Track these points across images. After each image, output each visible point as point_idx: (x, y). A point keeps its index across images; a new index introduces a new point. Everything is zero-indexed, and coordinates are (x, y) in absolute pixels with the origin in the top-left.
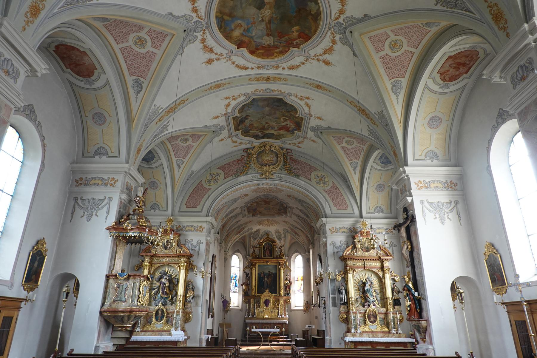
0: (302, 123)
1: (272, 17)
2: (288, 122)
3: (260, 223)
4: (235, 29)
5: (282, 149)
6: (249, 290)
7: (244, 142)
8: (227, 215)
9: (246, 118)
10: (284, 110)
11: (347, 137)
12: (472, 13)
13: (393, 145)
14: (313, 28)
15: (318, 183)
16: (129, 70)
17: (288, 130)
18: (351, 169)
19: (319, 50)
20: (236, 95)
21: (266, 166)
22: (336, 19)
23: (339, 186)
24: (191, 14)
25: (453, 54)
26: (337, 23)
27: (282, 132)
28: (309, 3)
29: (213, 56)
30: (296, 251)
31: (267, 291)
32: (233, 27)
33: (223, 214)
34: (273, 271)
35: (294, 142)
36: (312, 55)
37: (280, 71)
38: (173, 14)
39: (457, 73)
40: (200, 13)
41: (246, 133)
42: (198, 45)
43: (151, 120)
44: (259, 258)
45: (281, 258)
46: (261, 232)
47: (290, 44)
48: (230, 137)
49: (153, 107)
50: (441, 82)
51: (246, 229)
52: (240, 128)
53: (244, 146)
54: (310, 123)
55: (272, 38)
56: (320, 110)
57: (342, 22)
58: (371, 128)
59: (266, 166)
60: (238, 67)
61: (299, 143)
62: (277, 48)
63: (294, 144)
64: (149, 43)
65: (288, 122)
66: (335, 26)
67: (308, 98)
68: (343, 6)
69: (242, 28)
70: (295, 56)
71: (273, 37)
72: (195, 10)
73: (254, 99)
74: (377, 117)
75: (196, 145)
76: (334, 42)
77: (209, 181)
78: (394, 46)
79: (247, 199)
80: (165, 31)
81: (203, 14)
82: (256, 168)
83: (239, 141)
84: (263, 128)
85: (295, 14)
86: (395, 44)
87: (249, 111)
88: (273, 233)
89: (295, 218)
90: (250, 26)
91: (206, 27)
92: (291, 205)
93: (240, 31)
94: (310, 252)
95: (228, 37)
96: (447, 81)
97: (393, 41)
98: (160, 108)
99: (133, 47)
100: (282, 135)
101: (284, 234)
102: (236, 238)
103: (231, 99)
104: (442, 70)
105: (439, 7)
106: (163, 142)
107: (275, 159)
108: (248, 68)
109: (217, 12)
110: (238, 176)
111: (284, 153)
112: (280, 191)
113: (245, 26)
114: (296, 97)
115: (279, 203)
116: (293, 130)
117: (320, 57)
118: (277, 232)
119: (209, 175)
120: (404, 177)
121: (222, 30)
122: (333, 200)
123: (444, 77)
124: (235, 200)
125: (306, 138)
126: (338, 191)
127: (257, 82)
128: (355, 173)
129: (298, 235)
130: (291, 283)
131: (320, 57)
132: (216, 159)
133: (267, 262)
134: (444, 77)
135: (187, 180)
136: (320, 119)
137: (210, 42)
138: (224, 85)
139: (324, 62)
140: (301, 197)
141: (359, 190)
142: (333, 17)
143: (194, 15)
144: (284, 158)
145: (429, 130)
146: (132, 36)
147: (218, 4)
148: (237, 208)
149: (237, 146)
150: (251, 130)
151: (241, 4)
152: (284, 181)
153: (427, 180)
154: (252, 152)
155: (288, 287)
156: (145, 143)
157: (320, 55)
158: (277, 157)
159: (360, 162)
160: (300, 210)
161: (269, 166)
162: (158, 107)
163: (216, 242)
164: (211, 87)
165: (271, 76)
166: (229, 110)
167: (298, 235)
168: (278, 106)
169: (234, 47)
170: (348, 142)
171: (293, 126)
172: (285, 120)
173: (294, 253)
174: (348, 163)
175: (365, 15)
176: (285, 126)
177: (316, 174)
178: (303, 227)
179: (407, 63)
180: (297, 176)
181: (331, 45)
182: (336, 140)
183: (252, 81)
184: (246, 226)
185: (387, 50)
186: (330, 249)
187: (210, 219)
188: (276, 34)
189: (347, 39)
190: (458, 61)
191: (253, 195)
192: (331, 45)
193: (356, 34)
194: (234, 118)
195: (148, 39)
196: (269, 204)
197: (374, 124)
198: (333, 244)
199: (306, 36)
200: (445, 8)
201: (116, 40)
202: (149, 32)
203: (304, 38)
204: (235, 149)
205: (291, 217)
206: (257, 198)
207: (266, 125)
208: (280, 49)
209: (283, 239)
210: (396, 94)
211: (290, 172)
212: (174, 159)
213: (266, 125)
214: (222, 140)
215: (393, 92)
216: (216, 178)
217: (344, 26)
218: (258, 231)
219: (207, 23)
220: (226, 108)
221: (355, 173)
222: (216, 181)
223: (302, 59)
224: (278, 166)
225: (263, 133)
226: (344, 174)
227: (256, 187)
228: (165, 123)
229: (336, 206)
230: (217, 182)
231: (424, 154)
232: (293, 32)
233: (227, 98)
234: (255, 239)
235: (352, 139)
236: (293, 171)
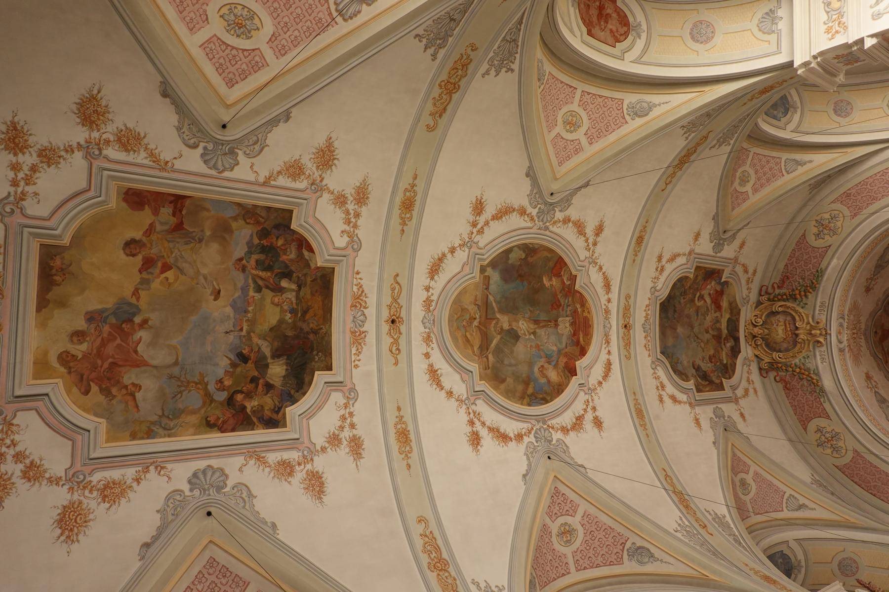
0: (705, 268)
1: (529, 318)
2: (705, 292)
4: (546, 377)
5: (759, 303)
7: (745, 375)
9: (698, 369)
10: (682, 301)
11: (732, 183)
12: (524, 13)
13: (749, 96)
14: (546, 254)
16: (611, 564)
17: (720, 293)
18: (801, 170)
19: (579, 243)
20: (655, 383)
21: (797, 335)
22: (532, 219)
23: (842, 190)
24: (525, 444)
25: (585, 30)
26: (538, 218)
27: (725, 304)
28: (510, 262)
29: (589, 416)
32: (543, 381)
35: (743, 282)
36: (587, 254)
37: (613, 307)
38: (525, 472)
39: (614, 15)
40: (524, 431)
41: (728, 370)
42: (571, 439)
43: (704, 543)
47: (570, 291)
48: (736, 401)
49: (679, 535)
50: (630, 38)
52: (717, 381)
53: (755, 376)
54: (707, 253)
55: (560, 319)
56: (682, 236)
57: (537, 210)
58: (715, 142)
59: (797, 335)
60: (606, 376)
61: (746, 271)
62: (575, 311)
63: (748, 282)
64: (568, 519)
65: (705, 292)
66: (542, 221)
67: (660, 258)
68: (514, 210)
69: (546, 365)
70: (589, 281)
71: (558, 317)
72: (519, 437)
73: (662, 353)
74: (693, 135)
75: (753, 468)
76: (566, 221)
77: (835, 449)
78: (572, 124)
79: (878, 376)
80: (550, 489)
81: (525, 425)
82: (804, 354)
83: (744, 384)
84: (718, 338)
85: (525, 283)
86: (569, 123)
87: (685, 363)
90: (542, 353)
91: (544, 424)
93: (550, 370)
95: (559, 389)
96: (629, 29)
97: (565, 127)
98: (680, 522)
99: (574, 547)
100: (730, 304)
103: (663, 393)
104: (611, 40)
105: (515, 66)
106: (750, 530)
107: (781, 318)
108: (609, 360)
109: (522, 404)
110: (823, 391)
111: (769, 300)
112: (855, 307)
113: (542, 362)
114: (658, 278)
116: (719, 283)
117: (591, 241)
119: (820, 449)
120: (818, 64)
121: (549, 398)
122: (875, 199)
123: (621, 35)
125: (736, 259)
126: (853, 191)
127: (632, 346)
128: (810, 162)
131: (591, 241)
132: (785, 433)
134: (621, 35)
135: (833, 494)
136: (697, 236)
137: (567, 419)
138: (637, 403)
139: (597, 235)
141: (849, 150)
142: (529, 225)
143: (526, 439)
144: (779, 300)
145: (718, 39)
146: (557, 545)
147: (510, 400)
149: (755, 390)
150: (721, 361)
151: (510, 365)
152: (832, 299)
153: (825, 17)
154: (767, 360)
156: (752, 565)
157: (587, 241)
158: (778, 313)
159: (785, 156)
161: (797, 328)
162: (679, 525)
164: (641, 426)
165: (621, 322)
166: (682, 397)
168: (675, 311)
169: (574, 381)
170: (744, 181)
171: (713, 283)
172: (701, 297)
174: (787, 177)
175: (528, 175)
176: (712, 299)
177: (813, 237)
179: (600, 100)
180: (819, 274)
181: (570, 224)
182: (739, 204)
183: (629, 354)
185: (579, 135)
188: (555, 312)
189: (561, 200)
190: (595, 19)
191: (868, 364)
192: (570, 224)
193: (555, 187)
194: (699, 391)
195: (561, 520)
197: (706, 138)
199: (558, 265)
200: (518, 56)
201: (563, 575)
202: (550, 517)
203: (561, 269)
204: (761, 393)
206: (875, 357)
207: (711, 332)
208: (578, 306)
210: (650, 109)
211: (812, 286)
212: (786, 514)
213: (711, 332)
214: (742, 415)
215: (647, 115)
217: (542, 207)
219: (538, 422)
220: (680, 402)
221: (810, 162)
223: (593, 271)
224: (796, 312)
225: (726, 339)
226: (812, 182)
227: (848, 355)
228: (710, 518)
230: (837, 434)
231: (766, 37)
232: (552, 285)
233: (661, 400)
235: (738, 174)
236: (808, 283)
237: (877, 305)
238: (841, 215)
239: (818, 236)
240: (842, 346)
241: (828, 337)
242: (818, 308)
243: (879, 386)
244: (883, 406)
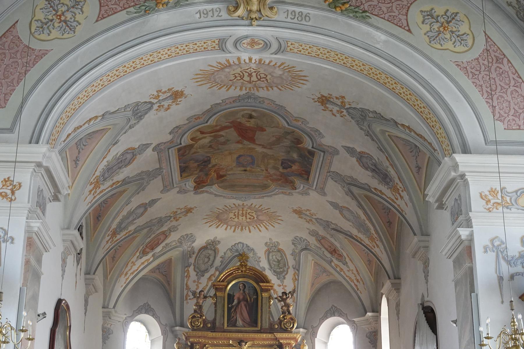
3: (219, 218)
8: (110, 170)
15: (434, 38)
23: (509, 52)
30: (333, 312)
33: (96, 161)
44: (213, 329)
45: (286, 331)
46: (222, 249)
51: (174, 237)
77: (44, 25)
79: (179, 114)
88: (261, 252)
89: (335, 191)
92: (327, 140)
94: (377, 310)
101: (296, 255)
102: (141, 265)
110: (147, 11)
112: (294, 77)
115: (287, 133)
118: (272, 249)
122: (490, 96)
124: (138, 111)
129: (340, 257)
140: (371, 96)
148: (144, 147)
160: (362, 158)
163: (71, 260)
167: (340, 257)
173: (325, 317)
178: (361, 227)
180: (361, 14)
186: (484, 266)
187: (40, 152)
191: (200, 99)
196: (252, 140)
198: (498, 248)
205: (322, 192)
206: (211, 112)
209: (291, 272)
216: (69, 15)
218: (211, 246)
222: (69, 26)
229: (501, 119)
230: (73, 29)
234: (201, 273)
237: (297, 119)
238: (461, 49)
239: (430, 14)
240: (229, 45)
241: (247, 22)
242: (298, 9)
243: (162, 113)
244: (129, 114)
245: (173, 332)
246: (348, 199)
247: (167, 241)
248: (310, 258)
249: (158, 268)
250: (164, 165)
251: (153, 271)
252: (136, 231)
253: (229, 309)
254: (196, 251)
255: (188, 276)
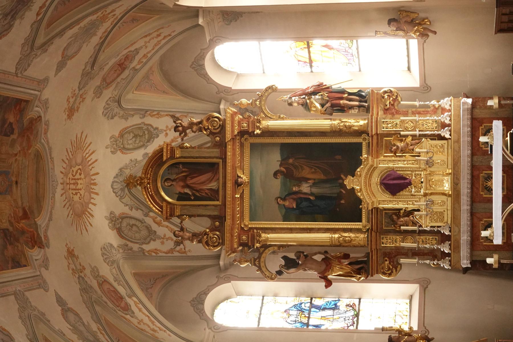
3: (80, 214)
6: (346, 256)
30: (198, 67)
31: (350, 182)
34: (274, 160)
44: (221, 218)
45: (223, 127)
46: (120, 209)
51: (106, 271)
88: (123, 159)
89: (42, 65)
101: (127, 115)
102: (143, 311)
118: (119, 145)
129: (129, 58)
130: (319, 89)
133: (238, 184)
155: (336, 101)
167: (129, 58)
173: (205, 76)
178: (89, 32)
184: (95, 271)
205: (43, 82)
209: (149, 120)
218: (117, 223)
234: (152, 235)
245: (226, 268)
246: (52, 48)
247: (111, 280)
248: (130, 96)
249: (146, 290)
250: (11, 289)
251: (150, 297)
252: (98, 320)
253: (197, 199)
254: (124, 241)
255: (156, 251)
